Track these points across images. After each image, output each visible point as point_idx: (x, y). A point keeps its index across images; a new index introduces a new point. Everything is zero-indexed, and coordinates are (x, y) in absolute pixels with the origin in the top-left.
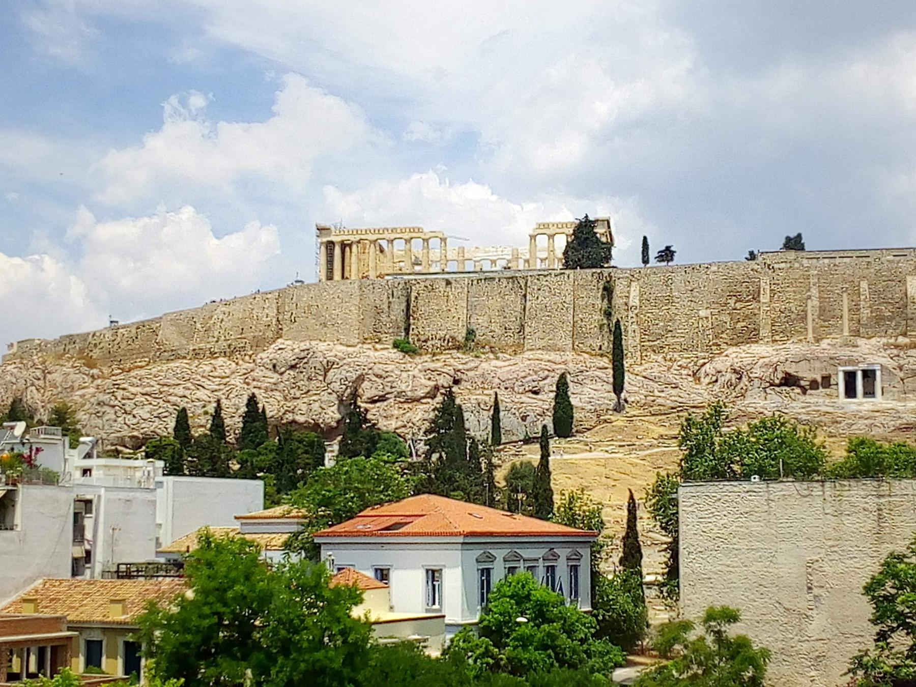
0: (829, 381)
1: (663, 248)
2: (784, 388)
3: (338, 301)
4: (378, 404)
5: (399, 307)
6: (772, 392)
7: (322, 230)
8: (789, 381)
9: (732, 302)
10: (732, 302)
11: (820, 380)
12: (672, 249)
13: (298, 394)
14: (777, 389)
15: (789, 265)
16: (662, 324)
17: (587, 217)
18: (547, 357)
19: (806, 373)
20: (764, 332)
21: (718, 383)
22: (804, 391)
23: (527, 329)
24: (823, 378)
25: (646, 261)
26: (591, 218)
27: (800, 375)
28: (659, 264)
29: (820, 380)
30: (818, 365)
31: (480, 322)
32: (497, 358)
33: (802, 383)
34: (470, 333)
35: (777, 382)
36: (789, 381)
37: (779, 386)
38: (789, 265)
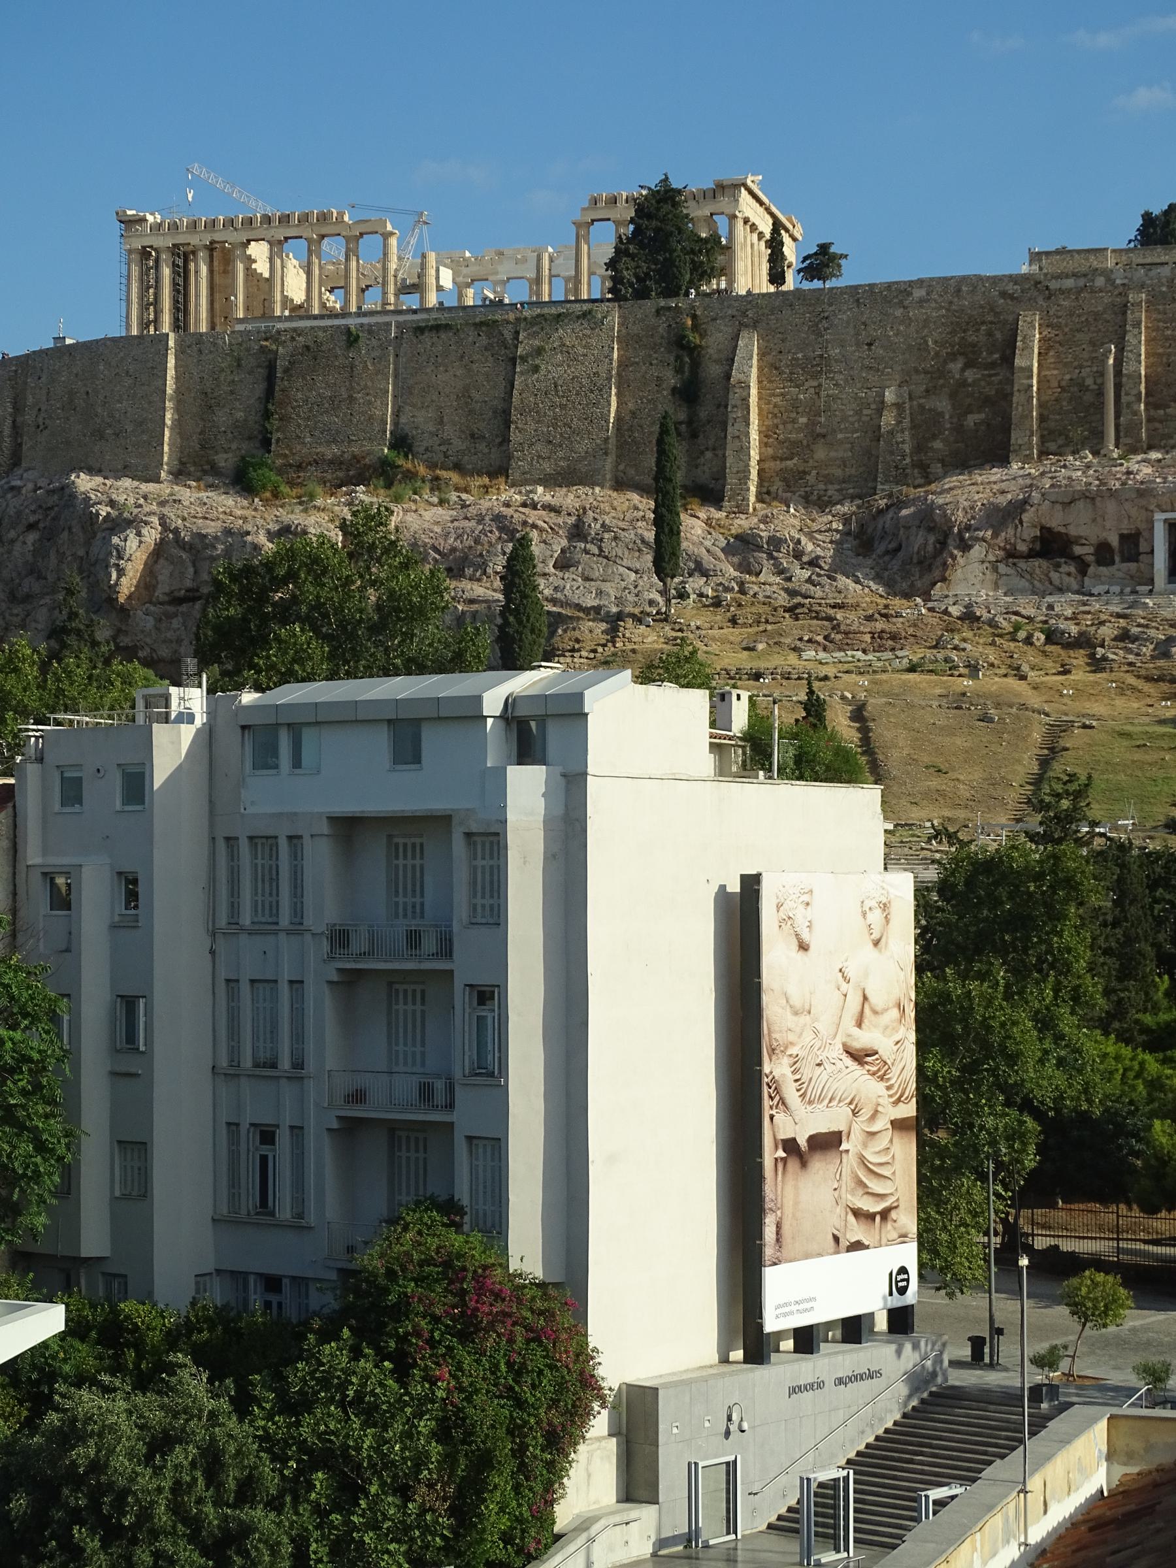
0: (1137, 545)
1: (814, 249)
2: (1036, 562)
3: (128, 382)
4: (184, 608)
5: (251, 390)
6: (1010, 571)
7: (129, 223)
8: (1052, 546)
9: (956, 367)
10: (956, 367)
11: (1114, 541)
12: (832, 250)
13: (37, 588)
14: (1022, 564)
15: (1081, 282)
16: (803, 420)
17: (667, 179)
18: (548, 498)
19: (1083, 527)
20: (1026, 435)
21: (901, 554)
22: (1083, 568)
23: (515, 437)
24: (1123, 537)
25: (777, 277)
26: (676, 184)
27: (1073, 531)
28: (807, 285)
29: (1114, 541)
30: (1111, 507)
31: (421, 420)
32: (442, 502)
33: (1078, 550)
34: (401, 443)
35: (1022, 547)
36: (1052, 546)
37: (1031, 555)
38: (1081, 282)
